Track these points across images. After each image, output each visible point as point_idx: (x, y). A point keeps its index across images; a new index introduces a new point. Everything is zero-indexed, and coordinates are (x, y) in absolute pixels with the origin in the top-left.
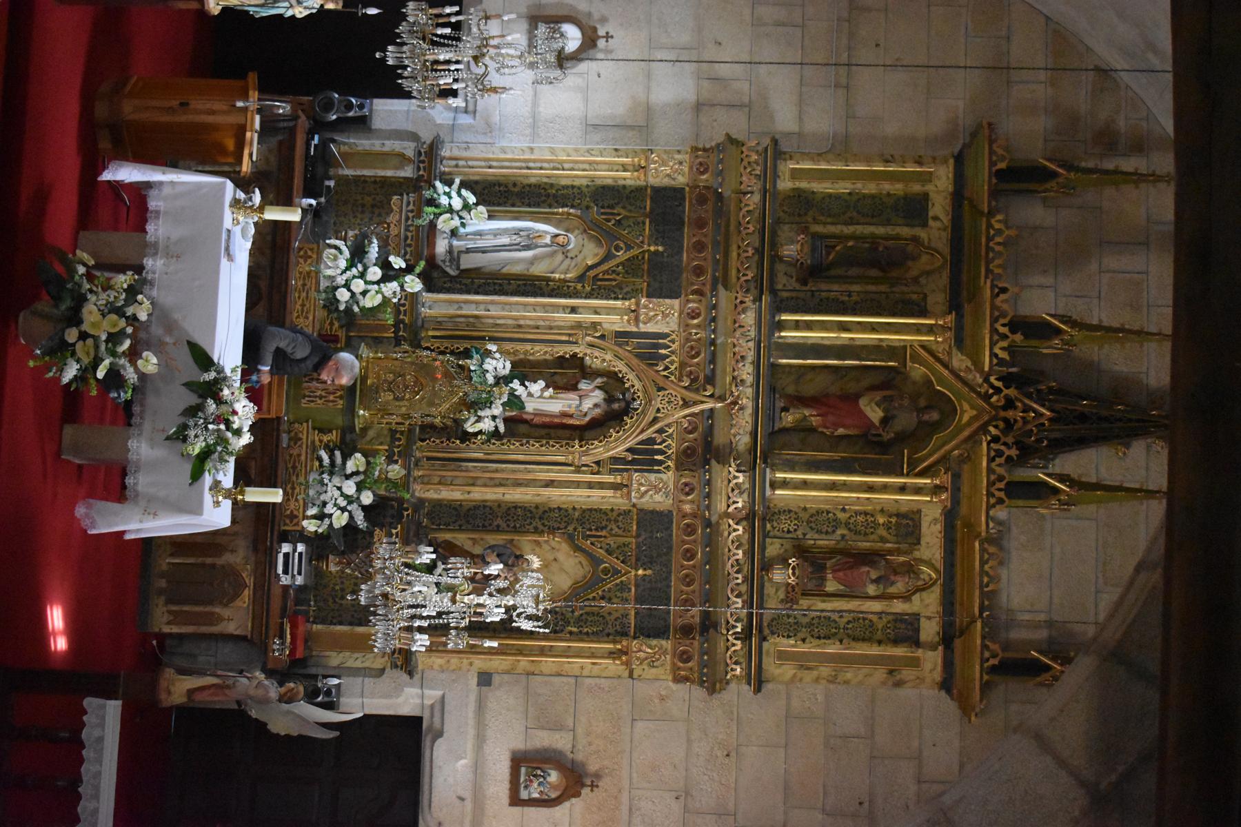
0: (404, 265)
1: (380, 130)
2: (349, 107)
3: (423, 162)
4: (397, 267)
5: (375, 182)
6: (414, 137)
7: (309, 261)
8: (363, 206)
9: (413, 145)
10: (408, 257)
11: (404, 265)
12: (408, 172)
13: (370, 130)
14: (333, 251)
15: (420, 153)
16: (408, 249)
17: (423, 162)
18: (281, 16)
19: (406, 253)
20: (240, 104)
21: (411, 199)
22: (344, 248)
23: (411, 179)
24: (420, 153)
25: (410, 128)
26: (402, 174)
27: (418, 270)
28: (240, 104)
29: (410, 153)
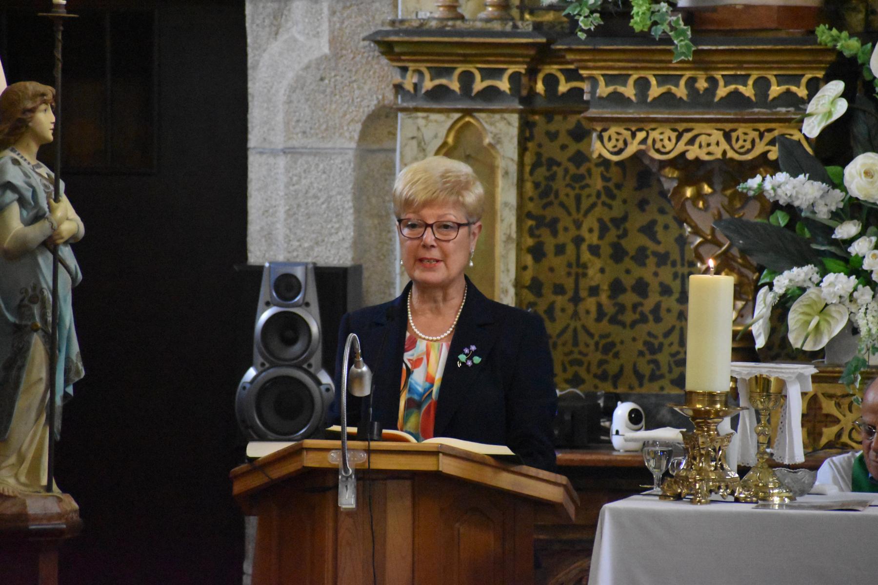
0: (837, 86)
1: (358, 244)
2: (287, 327)
3: (467, 79)
4: (842, 106)
5: (537, 252)
6: (380, 120)
7: (828, 407)
8: (617, 288)
9: (405, 126)
10: (802, 92)
11: (837, 86)
12: (502, 131)
13: (357, 269)
14: (794, 318)
15: (439, 93)
16: (775, 90)
17: (467, 79)
18: (77, 292)
19: (789, 99)
20: (348, 499)
21: (603, 90)
22: (783, 282)
23: (526, 126)
24: (439, 93)
25: (347, 141)
26: (508, 152)
27: (850, 45)
28: (348, 499)
29: (437, 126)
